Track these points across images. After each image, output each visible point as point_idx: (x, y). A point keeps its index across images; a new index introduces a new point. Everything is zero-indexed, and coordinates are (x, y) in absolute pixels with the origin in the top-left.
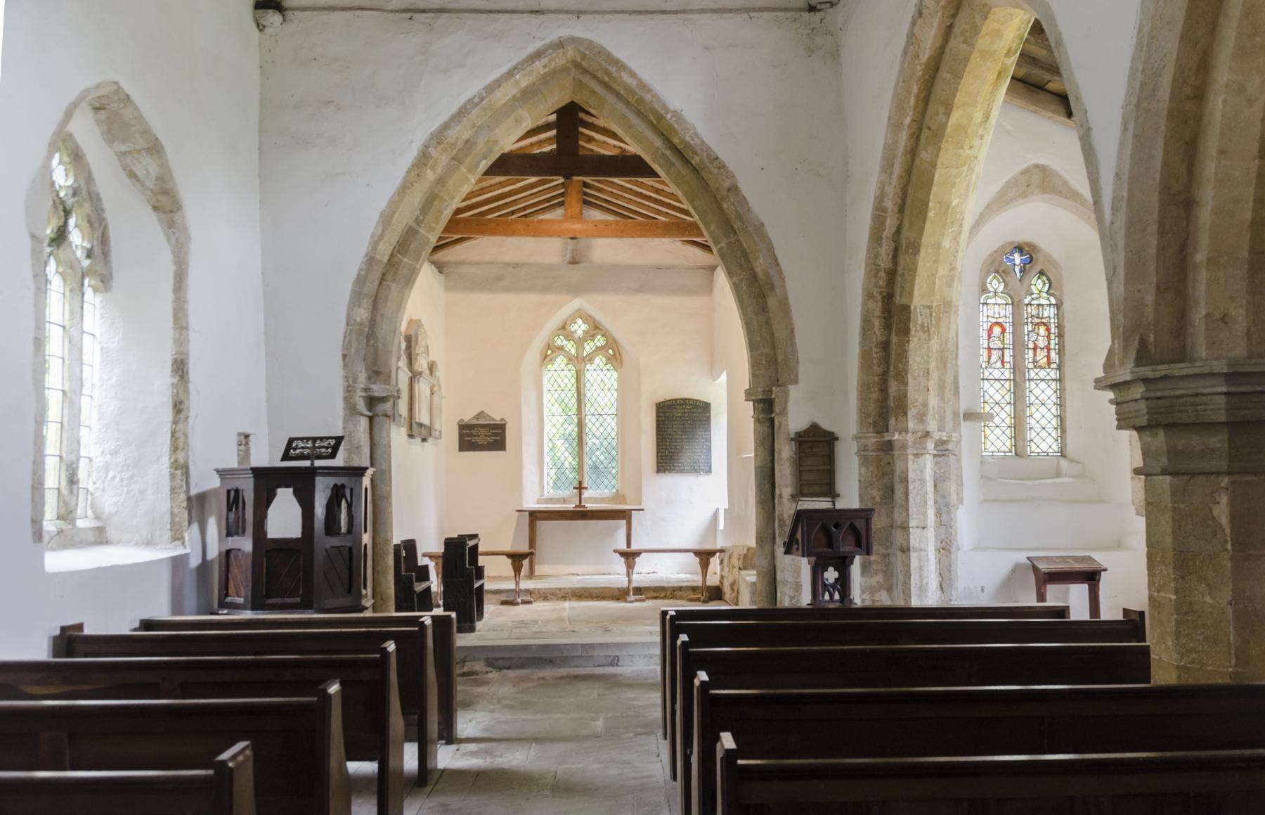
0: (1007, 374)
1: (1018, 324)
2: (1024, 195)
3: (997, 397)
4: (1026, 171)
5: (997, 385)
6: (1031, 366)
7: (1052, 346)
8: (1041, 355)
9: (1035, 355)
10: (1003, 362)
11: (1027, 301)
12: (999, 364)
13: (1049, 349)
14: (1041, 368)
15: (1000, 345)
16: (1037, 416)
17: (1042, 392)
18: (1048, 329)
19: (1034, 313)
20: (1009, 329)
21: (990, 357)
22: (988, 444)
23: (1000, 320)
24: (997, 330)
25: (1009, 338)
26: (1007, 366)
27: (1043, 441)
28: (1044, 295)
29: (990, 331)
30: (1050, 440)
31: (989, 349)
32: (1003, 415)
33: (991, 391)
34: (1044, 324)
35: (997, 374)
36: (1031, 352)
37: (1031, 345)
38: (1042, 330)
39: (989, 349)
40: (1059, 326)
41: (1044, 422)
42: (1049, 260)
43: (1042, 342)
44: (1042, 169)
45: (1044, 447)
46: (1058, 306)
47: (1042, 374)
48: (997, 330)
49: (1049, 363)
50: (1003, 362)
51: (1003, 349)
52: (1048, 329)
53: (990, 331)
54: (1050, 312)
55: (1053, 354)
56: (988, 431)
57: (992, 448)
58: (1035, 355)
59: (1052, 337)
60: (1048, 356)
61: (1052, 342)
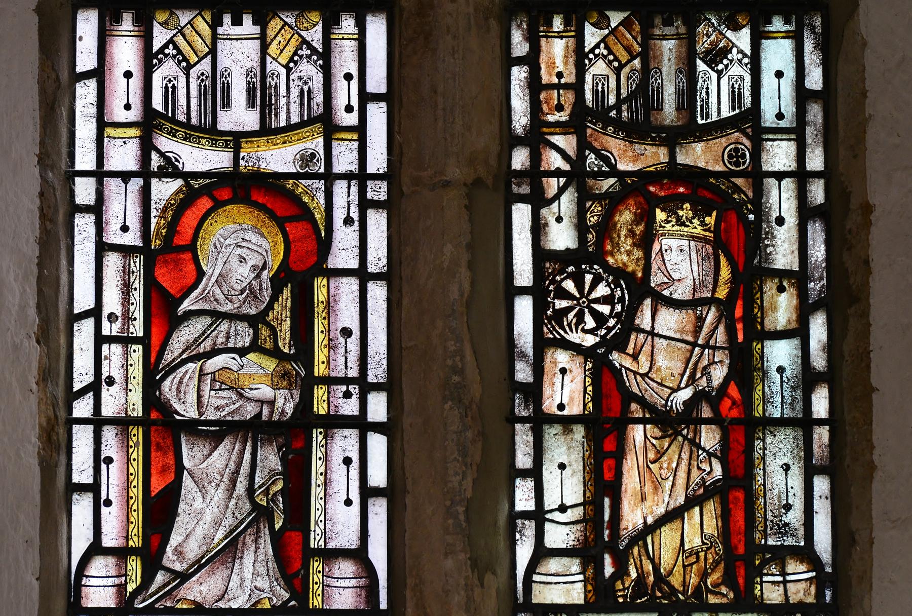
9: (603, 483)
13: (743, 431)
15: (261, 385)
18: (738, 240)
20: (360, 239)
21: (160, 511)
23: (278, 158)
24: (237, 252)
25: (355, 319)
37: (567, 389)
38: (680, 260)
39: (160, 429)
40: (840, 213)
43: (666, 358)
48: (237, 252)
51: (294, 436)
52: (738, 240)
55: (780, 469)
58: (603, 483)
59: (782, 308)
60: (736, 488)
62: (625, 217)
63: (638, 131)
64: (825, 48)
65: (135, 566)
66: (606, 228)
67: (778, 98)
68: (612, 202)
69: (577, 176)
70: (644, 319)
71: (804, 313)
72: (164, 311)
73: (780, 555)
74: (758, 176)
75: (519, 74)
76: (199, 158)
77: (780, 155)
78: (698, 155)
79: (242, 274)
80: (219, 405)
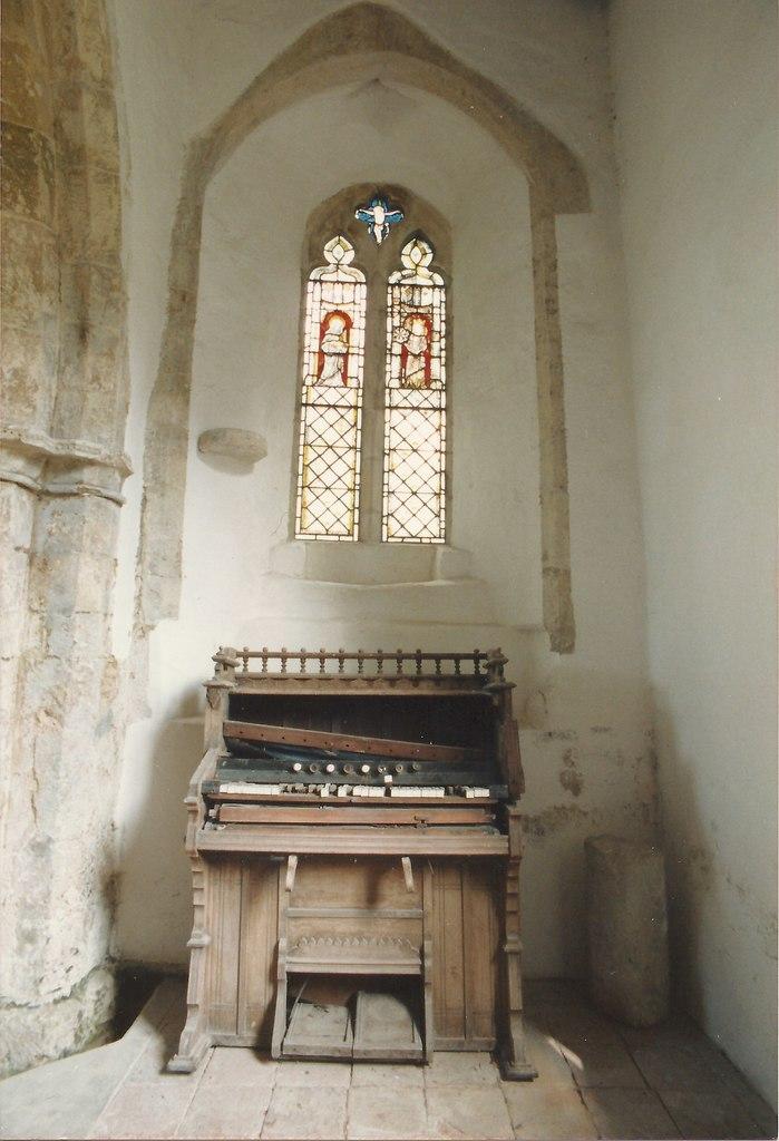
0: (352, 397)
1: (377, 313)
2: (341, 50)
3: (331, 437)
4: (347, 14)
5: (332, 415)
6: (395, 383)
7: (435, 352)
8: (414, 366)
9: (403, 365)
10: (345, 377)
11: (393, 279)
12: (338, 380)
13: (428, 357)
14: (412, 387)
15: (341, 348)
16: (403, 471)
17: (416, 432)
18: (429, 326)
19: (405, 298)
20: (359, 322)
21: (321, 368)
22: (309, 519)
24: (337, 324)
25: (358, 337)
26: (352, 383)
27: (414, 514)
28: (423, 271)
29: (324, 326)
30: (426, 515)
31: (322, 354)
32: (340, 468)
33: (320, 426)
34: (422, 316)
35: (331, 397)
36: (396, 362)
37: (397, 349)
38: (419, 327)
39: (322, 354)
40: (448, 321)
41: (415, 483)
42: (429, 211)
43: (416, 346)
44: (379, 12)
45: (414, 527)
46: (446, 288)
47: (416, 398)
48: (337, 324)
49: (428, 380)
50: (345, 377)
51: (345, 356)
52: (429, 326)
53: (324, 326)
54: (436, 298)
55: (435, 363)
56: (309, 496)
57: (316, 528)
58: (403, 365)
59: (436, 337)
60: (427, 369)
61: (436, 347)
62: (408, 320)
63: (411, 306)
64: (446, 293)
65: (315, 378)
66: (404, 323)
67: (436, 303)
68: (406, 318)
69: (399, 312)
70: (411, 338)
71: (441, 338)
72: (323, 334)
73: (435, 380)
74: (432, 314)
75: (389, 296)
76: (332, 308)
77: (436, 311)
78: (421, 311)
79: (337, 328)
80: (332, 350)
